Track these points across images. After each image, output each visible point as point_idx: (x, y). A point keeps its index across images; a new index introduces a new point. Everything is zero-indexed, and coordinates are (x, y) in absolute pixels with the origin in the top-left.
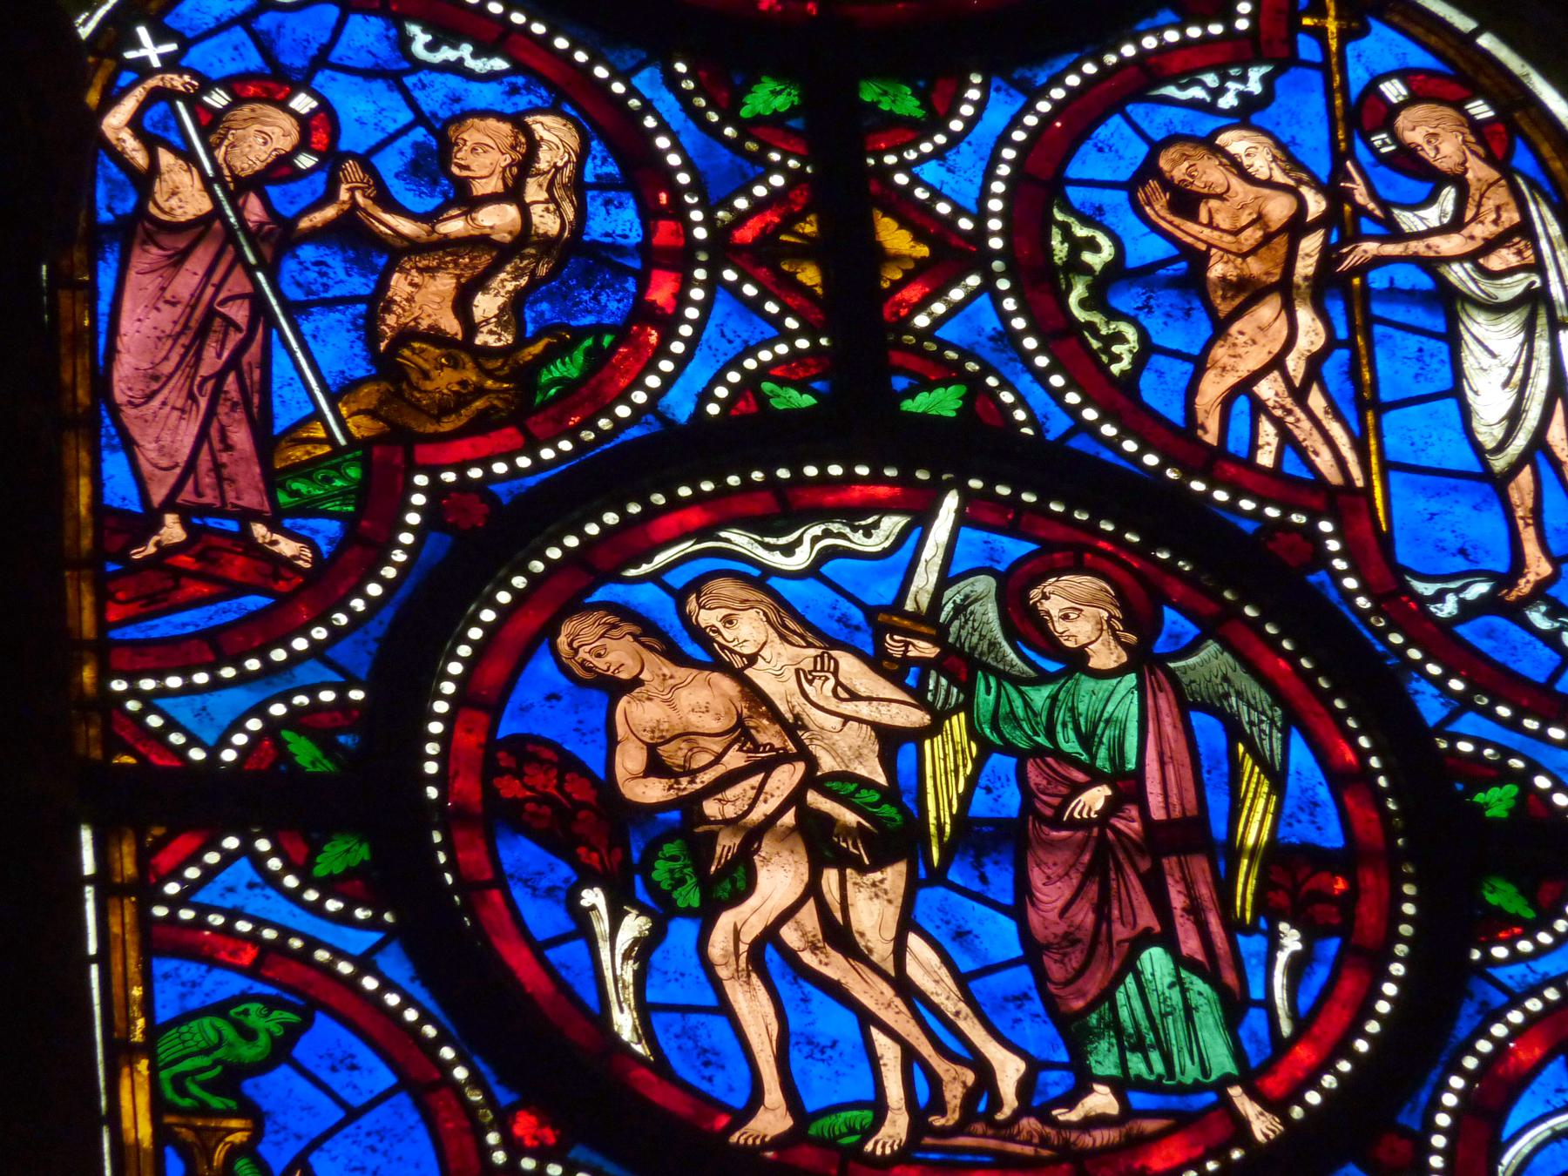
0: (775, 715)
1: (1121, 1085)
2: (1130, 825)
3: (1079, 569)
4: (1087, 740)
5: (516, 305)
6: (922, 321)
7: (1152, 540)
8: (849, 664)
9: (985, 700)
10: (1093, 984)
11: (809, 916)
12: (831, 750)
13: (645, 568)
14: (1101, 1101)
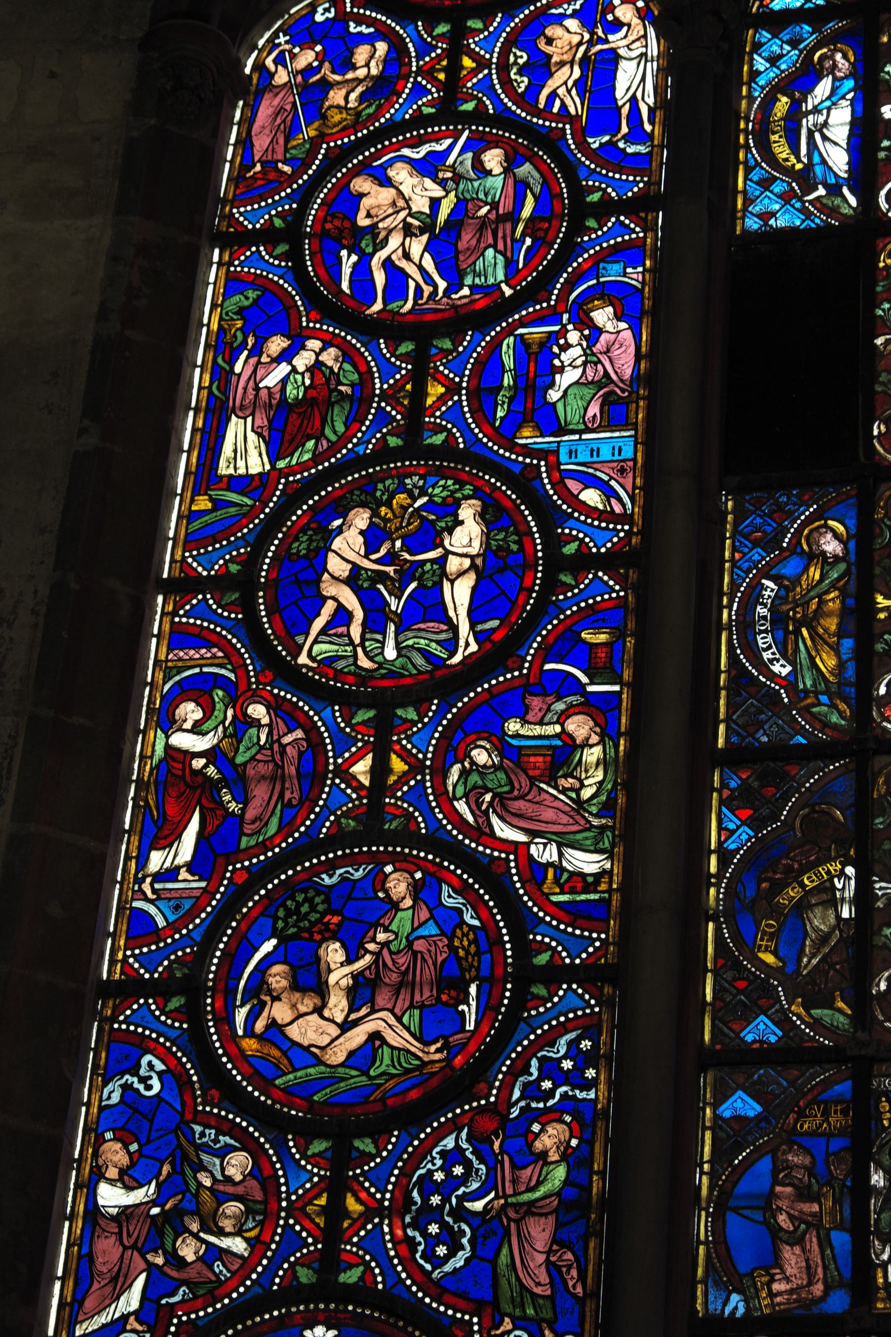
0: (404, 198)
1: (473, 288)
2: (493, 216)
3: (497, 147)
4: (486, 195)
5: (362, 98)
6: (469, 85)
7: (518, 137)
8: (428, 182)
9: (461, 187)
10: (470, 261)
11: (400, 252)
12: (417, 206)
13: (379, 162)
14: (466, 291)
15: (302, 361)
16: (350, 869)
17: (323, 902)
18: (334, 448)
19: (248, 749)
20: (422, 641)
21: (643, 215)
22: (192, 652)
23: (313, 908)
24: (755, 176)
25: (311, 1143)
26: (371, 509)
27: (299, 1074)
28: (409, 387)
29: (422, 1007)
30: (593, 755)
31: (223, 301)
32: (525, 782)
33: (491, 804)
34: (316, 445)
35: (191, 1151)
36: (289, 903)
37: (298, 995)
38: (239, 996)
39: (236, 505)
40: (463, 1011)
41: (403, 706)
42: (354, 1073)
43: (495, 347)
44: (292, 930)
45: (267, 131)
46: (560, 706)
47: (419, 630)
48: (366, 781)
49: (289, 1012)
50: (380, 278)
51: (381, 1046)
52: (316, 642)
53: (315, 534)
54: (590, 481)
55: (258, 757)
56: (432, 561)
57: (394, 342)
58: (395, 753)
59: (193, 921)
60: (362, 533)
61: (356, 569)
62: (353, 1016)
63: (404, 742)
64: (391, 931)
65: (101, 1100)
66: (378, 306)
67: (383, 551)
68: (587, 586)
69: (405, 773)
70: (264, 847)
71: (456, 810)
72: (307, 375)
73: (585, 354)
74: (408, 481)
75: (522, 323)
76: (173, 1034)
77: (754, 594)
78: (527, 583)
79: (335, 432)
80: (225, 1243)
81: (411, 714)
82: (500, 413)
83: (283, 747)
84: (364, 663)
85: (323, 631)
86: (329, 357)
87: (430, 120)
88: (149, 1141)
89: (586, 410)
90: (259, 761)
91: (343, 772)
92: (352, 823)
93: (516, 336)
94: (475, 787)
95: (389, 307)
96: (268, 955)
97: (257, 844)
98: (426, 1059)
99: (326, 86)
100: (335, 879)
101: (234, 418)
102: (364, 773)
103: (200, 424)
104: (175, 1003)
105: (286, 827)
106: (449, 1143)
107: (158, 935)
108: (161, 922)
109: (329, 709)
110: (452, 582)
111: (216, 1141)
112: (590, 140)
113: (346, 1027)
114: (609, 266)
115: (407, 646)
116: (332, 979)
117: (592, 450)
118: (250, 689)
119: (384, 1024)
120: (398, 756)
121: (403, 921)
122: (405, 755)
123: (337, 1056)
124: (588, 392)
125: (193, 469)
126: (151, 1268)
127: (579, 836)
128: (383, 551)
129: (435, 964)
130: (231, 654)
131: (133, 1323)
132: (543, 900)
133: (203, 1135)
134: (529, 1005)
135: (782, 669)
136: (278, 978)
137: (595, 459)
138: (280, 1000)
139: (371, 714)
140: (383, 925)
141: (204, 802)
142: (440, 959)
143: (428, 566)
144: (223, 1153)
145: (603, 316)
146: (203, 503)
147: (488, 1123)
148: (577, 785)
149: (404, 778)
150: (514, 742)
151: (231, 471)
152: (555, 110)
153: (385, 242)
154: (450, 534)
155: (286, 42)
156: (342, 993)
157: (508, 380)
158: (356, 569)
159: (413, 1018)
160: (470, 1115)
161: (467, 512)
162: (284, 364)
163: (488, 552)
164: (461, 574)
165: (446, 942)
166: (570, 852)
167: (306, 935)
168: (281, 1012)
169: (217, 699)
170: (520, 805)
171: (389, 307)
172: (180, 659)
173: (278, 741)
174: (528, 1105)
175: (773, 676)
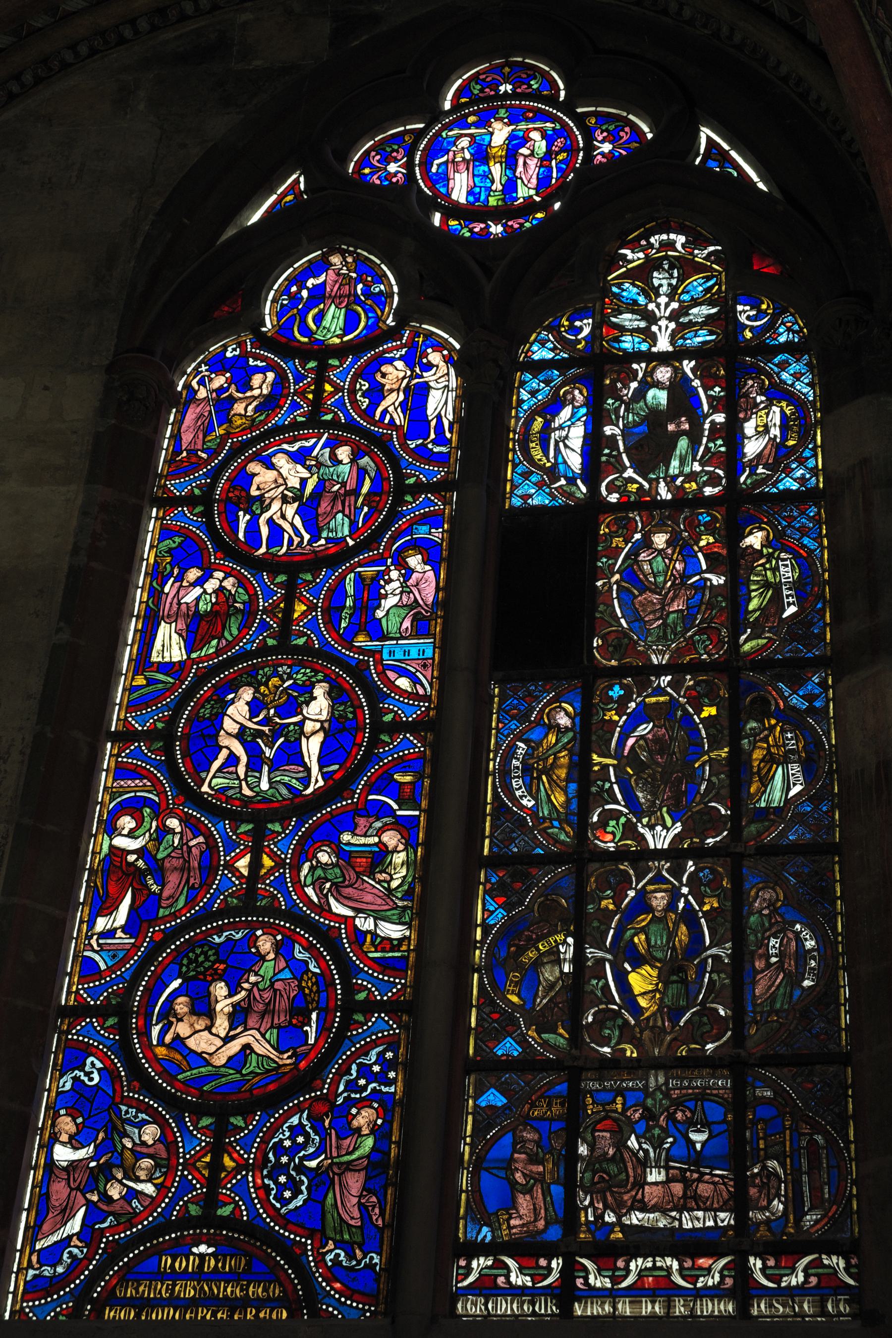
0: (283, 477)
1: (328, 540)
2: (342, 491)
4: (338, 477)
5: (256, 409)
6: (329, 403)
7: (361, 439)
8: (299, 468)
9: (322, 471)
10: (326, 521)
11: (279, 514)
14: (323, 542)
15: (211, 585)
16: (233, 932)
17: (214, 955)
18: (230, 645)
19: (166, 849)
20: (286, 778)
21: (443, 493)
22: (130, 782)
23: (207, 959)
24: (519, 470)
25: (201, 1119)
26: (254, 687)
27: (194, 1072)
28: (282, 605)
29: (279, 1027)
30: (399, 858)
31: (158, 544)
32: (353, 875)
33: (330, 890)
34: (218, 643)
35: (119, 1123)
36: (191, 954)
37: (195, 1018)
38: (155, 1018)
39: (163, 682)
40: (307, 1031)
41: (272, 822)
42: (232, 1071)
43: (341, 580)
44: (192, 973)
45: (191, 430)
46: (378, 824)
47: (285, 770)
48: (245, 872)
49: (189, 1029)
50: (265, 531)
51: (250, 1054)
52: (214, 777)
53: (216, 703)
54: (403, 673)
55: (172, 854)
56: (295, 724)
57: (273, 574)
58: (266, 854)
59: (124, 966)
60: (247, 703)
61: (243, 728)
62: (232, 1033)
63: (272, 846)
65: (58, 1087)
66: (263, 550)
67: (261, 717)
68: (399, 743)
69: (272, 868)
70: (174, 916)
71: (306, 894)
72: (213, 596)
73: (402, 587)
74: (280, 669)
75: (360, 565)
76: (109, 1043)
77: (511, 752)
78: (358, 740)
79: (231, 635)
80: (140, 1187)
81: (277, 827)
82: (343, 625)
83: (190, 848)
84: (247, 792)
85: (219, 770)
86: (229, 584)
87: (302, 425)
88: (90, 1117)
89: (401, 624)
90: (173, 857)
91: (230, 866)
92: (235, 901)
93: (355, 573)
94: (319, 878)
95: (270, 551)
96: (176, 990)
97: (170, 914)
98: (281, 1063)
99: (232, 400)
100: (222, 939)
101: (162, 622)
102: (244, 867)
103: (140, 626)
104: (111, 1022)
105: (191, 902)
106: (295, 1120)
107: (101, 975)
108: (103, 966)
109: (222, 823)
110: (308, 738)
111: (136, 1117)
112: (409, 442)
113: (227, 1040)
114: (419, 527)
115: (276, 781)
116: (219, 1007)
117: (405, 651)
118: (168, 808)
120: (268, 856)
121: (267, 969)
122: (272, 855)
123: (220, 1060)
124: (403, 612)
125: (134, 657)
126: (89, 1203)
127: (389, 913)
128: (261, 717)
129: (288, 999)
130: (155, 782)
131: (75, 1241)
132: (363, 955)
133: (127, 1112)
134: (352, 1027)
135: (528, 802)
136: (181, 1006)
137: (407, 657)
138: (183, 1021)
139: (250, 826)
140: (254, 971)
141: (135, 884)
142: (292, 995)
143: (292, 727)
144: (140, 1125)
145: (414, 561)
146: (140, 681)
147: (321, 1108)
148: (388, 878)
149: (271, 871)
150: (347, 848)
151: (160, 659)
152: (386, 421)
153: (269, 506)
154: (307, 706)
155: (206, 370)
156: (225, 1017)
157: (349, 602)
158: (243, 728)
159: (272, 1035)
160: (309, 1102)
161: (319, 691)
162: (198, 588)
163: (332, 719)
164: (314, 733)
166: (381, 923)
167: (202, 977)
168: (183, 1029)
169: (145, 815)
170: (350, 890)
171: (270, 551)
172: (121, 787)
173: (187, 844)
174: (349, 1095)
175: (522, 807)
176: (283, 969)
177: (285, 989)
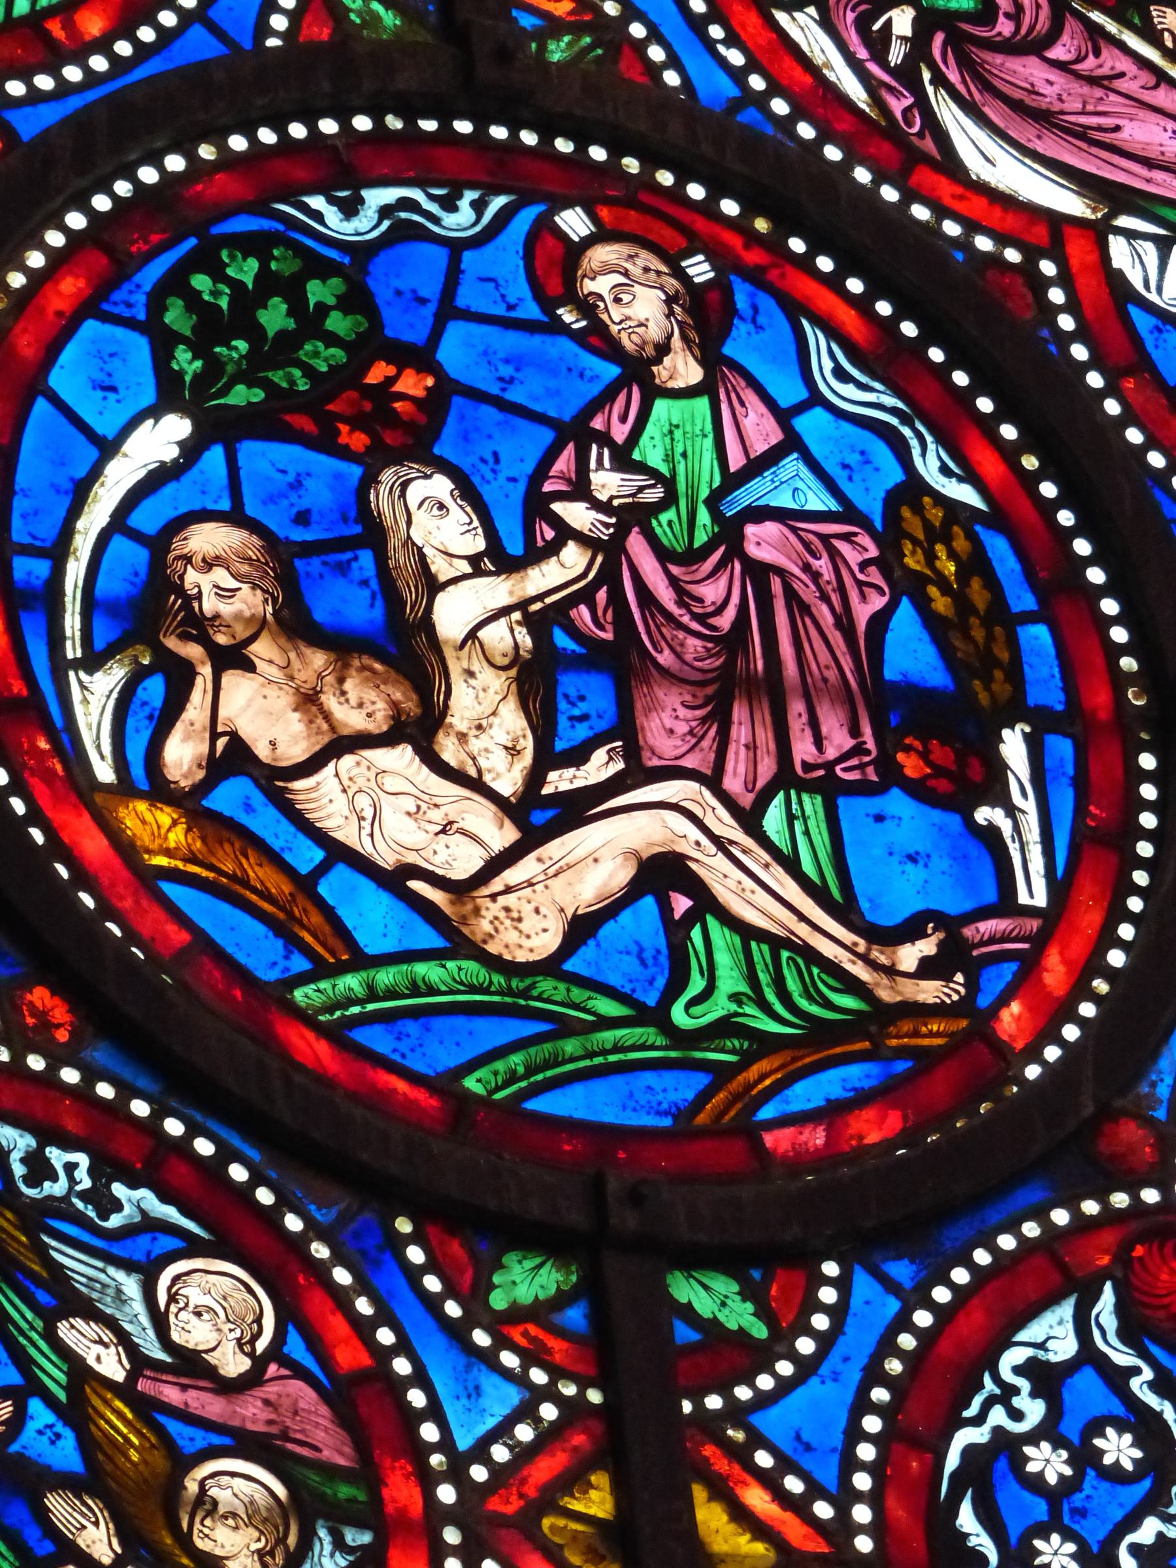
16: (416, 194)
17: (345, 304)
42: (608, 1007)
51: (694, 916)
62: (559, 781)
64: (642, 468)
119: (695, 833)
140: (604, 439)
142: (863, 613)
156: (494, 682)
165: (873, 552)
176: (772, 457)
177: (816, 576)
